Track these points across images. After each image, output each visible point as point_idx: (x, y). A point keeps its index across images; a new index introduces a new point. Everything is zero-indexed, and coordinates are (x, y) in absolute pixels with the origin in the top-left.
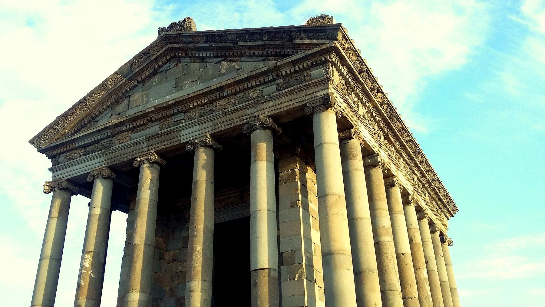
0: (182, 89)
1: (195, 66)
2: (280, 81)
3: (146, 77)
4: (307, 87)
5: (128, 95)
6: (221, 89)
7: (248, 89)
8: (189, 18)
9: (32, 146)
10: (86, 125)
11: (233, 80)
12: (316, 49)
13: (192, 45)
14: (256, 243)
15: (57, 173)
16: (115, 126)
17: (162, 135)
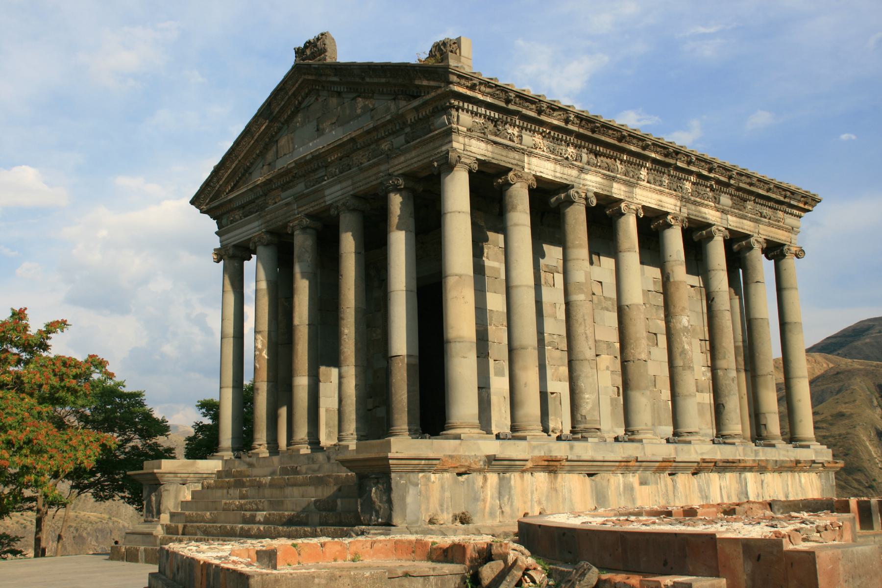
0: (323, 134)
1: (334, 101)
2: (408, 130)
3: (289, 116)
4: (433, 139)
5: (275, 139)
6: (352, 140)
7: (379, 139)
8: (322, 34)
9: (193, 207)
10: (240, 178)
11: (360, 131)
12: (433, 94)
13: (324, 78)
14: (446, 303)
15: (224, 237)
16: (265, 183)
17: (308, 195)
